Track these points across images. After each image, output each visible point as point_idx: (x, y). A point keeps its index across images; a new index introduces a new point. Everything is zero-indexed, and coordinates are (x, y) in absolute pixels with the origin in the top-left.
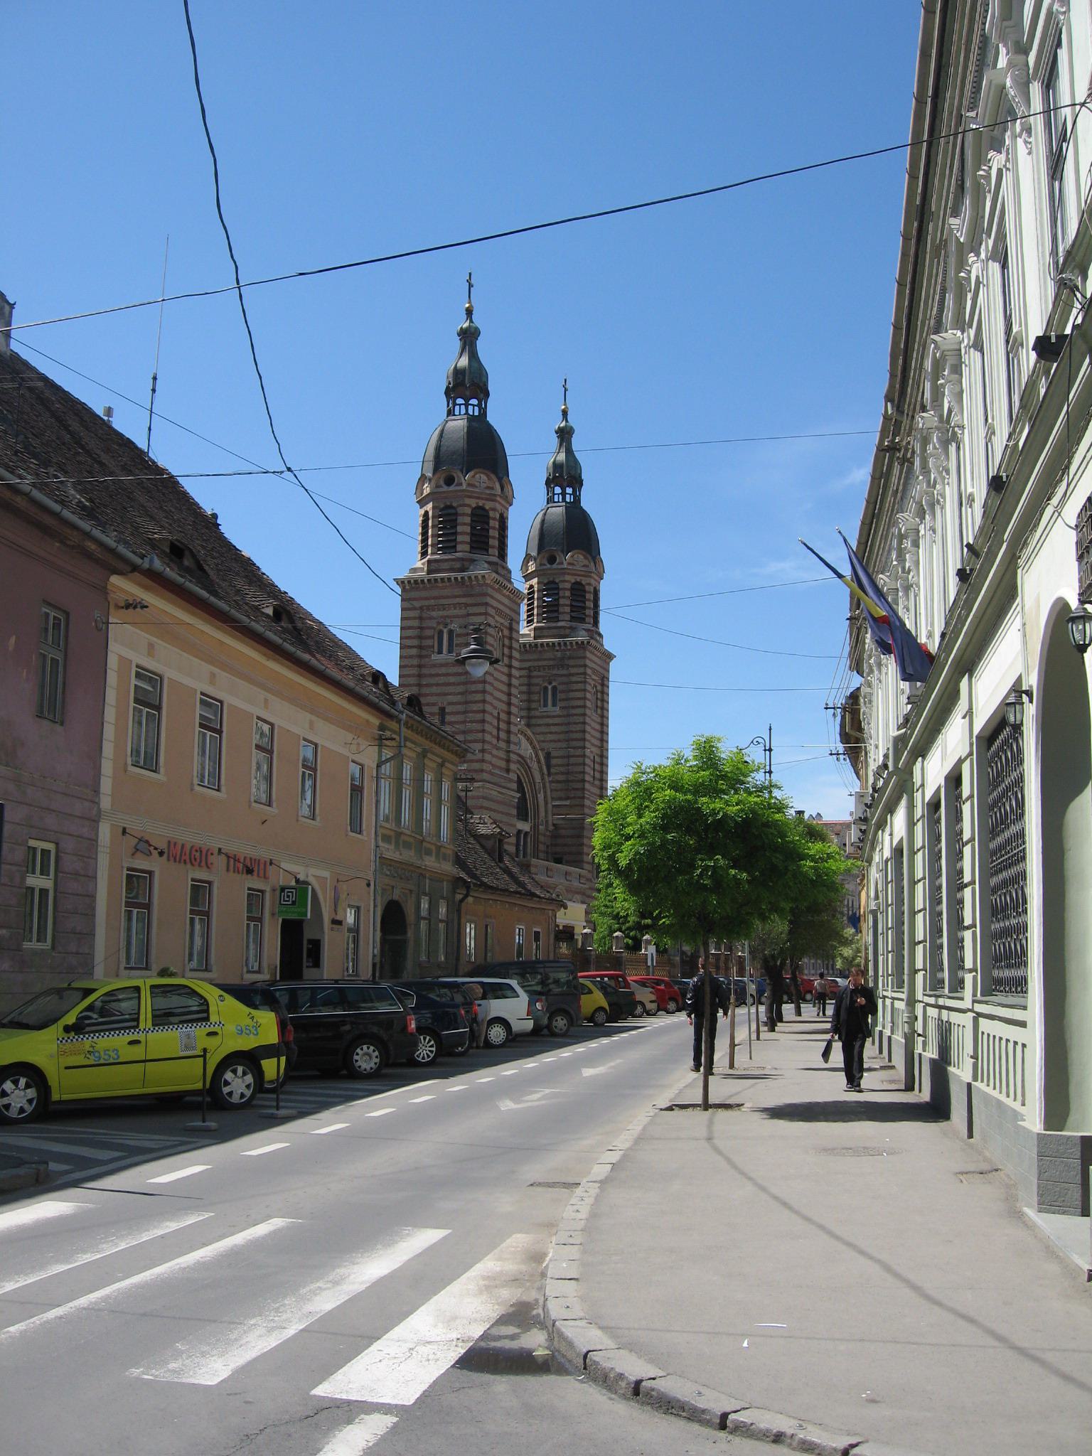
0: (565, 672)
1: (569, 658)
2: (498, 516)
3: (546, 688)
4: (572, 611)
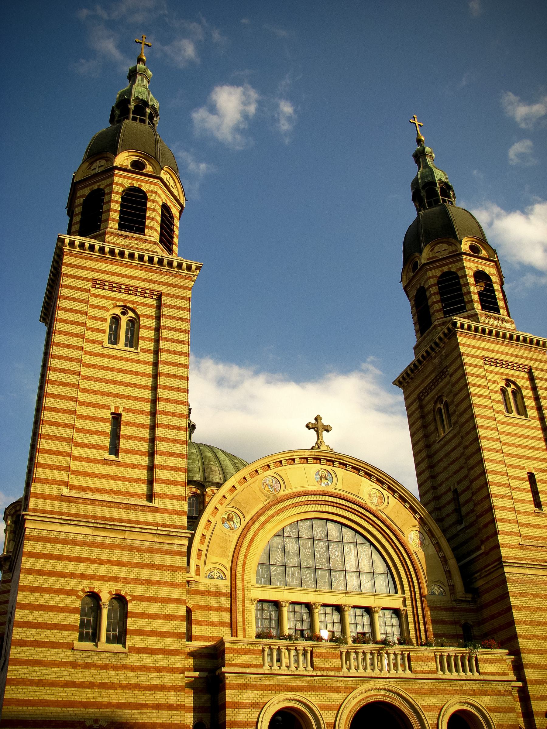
1: (447, 356)
3: (440, 410)
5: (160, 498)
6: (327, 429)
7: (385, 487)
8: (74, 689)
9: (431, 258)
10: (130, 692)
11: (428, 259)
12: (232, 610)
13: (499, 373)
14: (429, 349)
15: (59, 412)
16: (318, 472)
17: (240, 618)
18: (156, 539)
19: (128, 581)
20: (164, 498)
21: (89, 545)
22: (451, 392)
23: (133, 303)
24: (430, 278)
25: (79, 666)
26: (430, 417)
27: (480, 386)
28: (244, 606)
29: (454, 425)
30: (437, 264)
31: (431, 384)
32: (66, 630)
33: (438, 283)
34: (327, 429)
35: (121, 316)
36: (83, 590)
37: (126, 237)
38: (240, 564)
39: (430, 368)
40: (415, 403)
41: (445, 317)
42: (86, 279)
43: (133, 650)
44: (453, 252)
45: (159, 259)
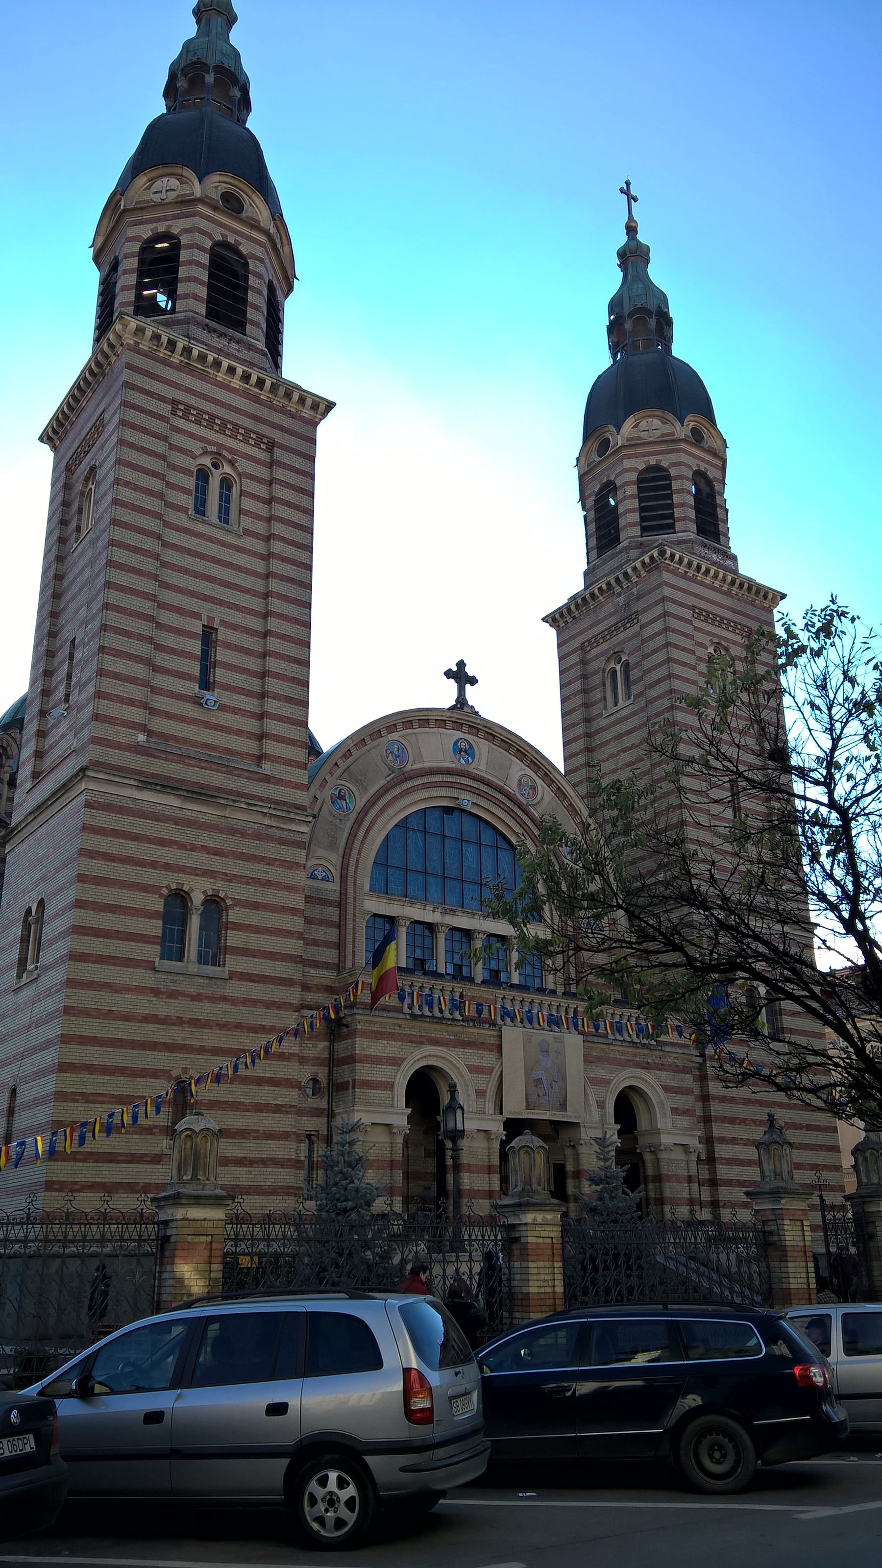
1: (640, 597)
3: (614, 672)
4: (643, 519)
5: (273, 762)
6: (473, 681)
7: (540, 774)
8: (156, 1026)
9: (632, 439)
10: (229, 1033)
11: (628, 439)
12: (340, 926)
13: (709, 633)
14: (613, 582)
15: (130, 615)
16: (456, 743)
17: (350, 938)
18: (267, 821)
19: (230, 878)
20: (278, 762)
21: (176, 821)
22: (638, 649)
23: (231, 451)
24: (626, 470)
25: (162, 993)
26: (597, 679)
27: (684, 649)
28: (354, 921)
29: (637, 696)
30: (640, 450)
31: (606, 633)
32: (146, 942)
33: (640, 481)
34: (473, 681)
35: (213, 469)
36: (167, 887)
37: (222, 335)
38: (353, 861)
39: (608, 608)
40: (575, 655)
41: (642, 536)
42: (162, 399)
43: (233, 975)
44: (668, 435)
45: (272, 383)
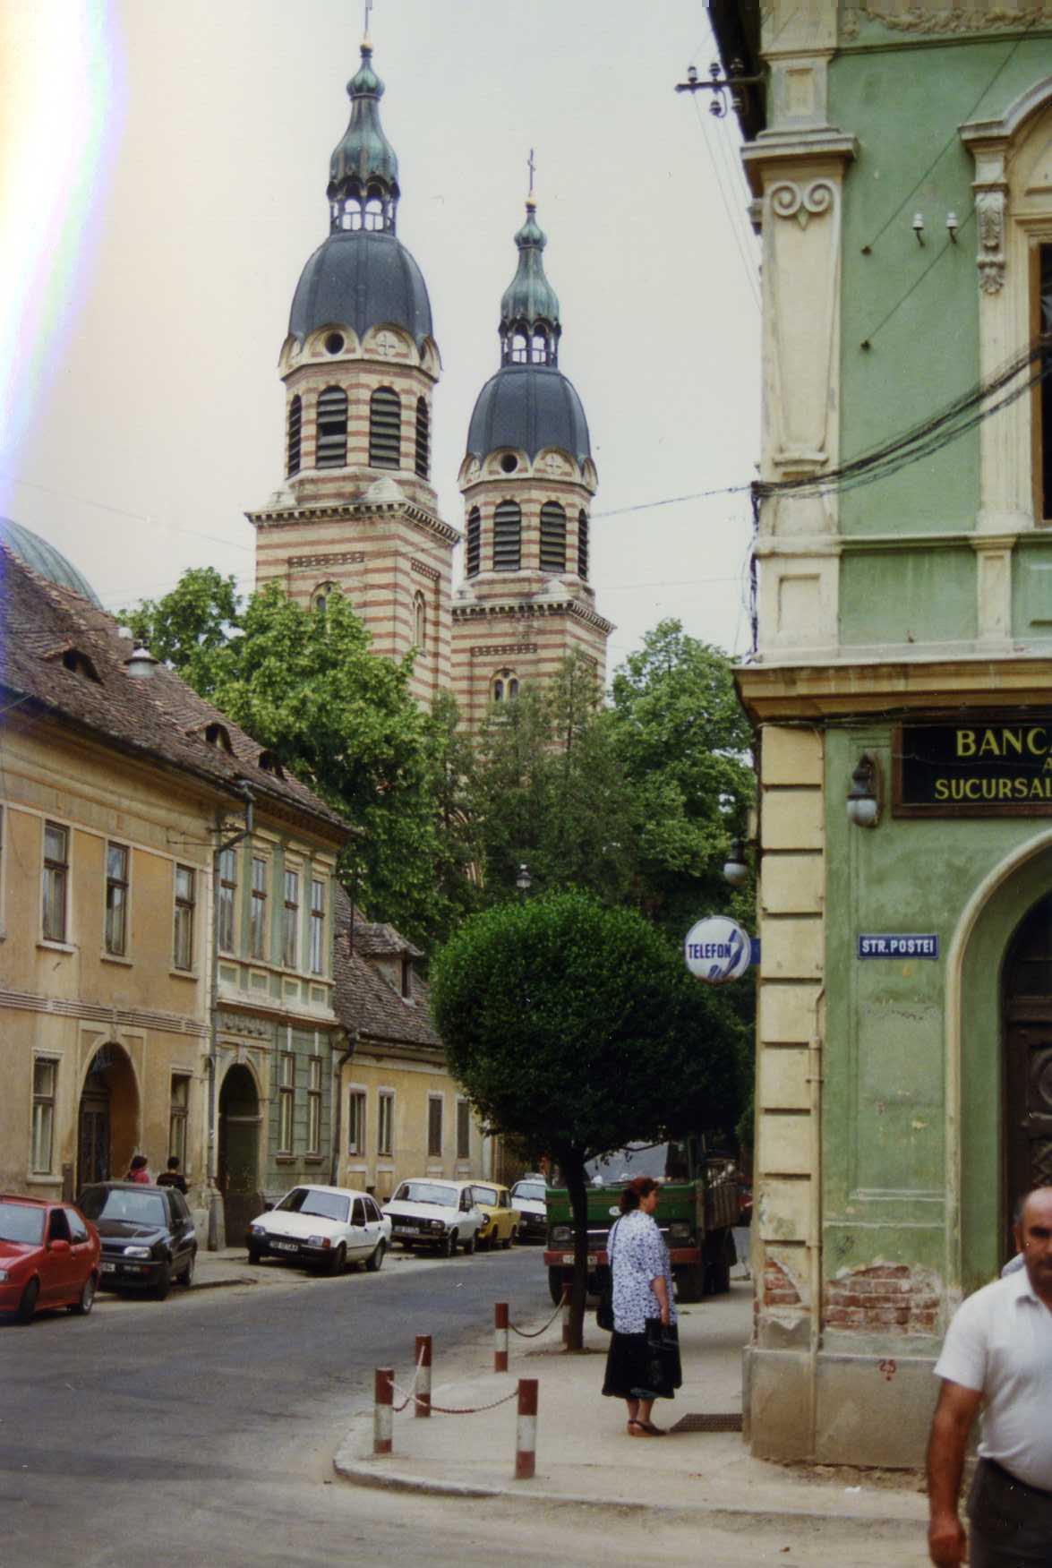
0: (530, 656)
1: (541, 632)
2: (414, 402)
3: (499, 683)
